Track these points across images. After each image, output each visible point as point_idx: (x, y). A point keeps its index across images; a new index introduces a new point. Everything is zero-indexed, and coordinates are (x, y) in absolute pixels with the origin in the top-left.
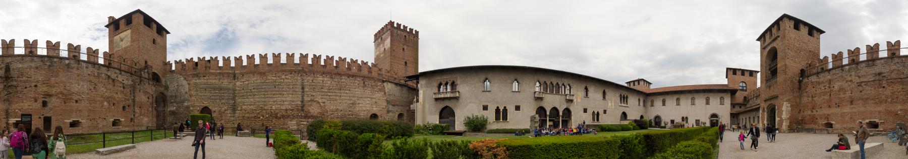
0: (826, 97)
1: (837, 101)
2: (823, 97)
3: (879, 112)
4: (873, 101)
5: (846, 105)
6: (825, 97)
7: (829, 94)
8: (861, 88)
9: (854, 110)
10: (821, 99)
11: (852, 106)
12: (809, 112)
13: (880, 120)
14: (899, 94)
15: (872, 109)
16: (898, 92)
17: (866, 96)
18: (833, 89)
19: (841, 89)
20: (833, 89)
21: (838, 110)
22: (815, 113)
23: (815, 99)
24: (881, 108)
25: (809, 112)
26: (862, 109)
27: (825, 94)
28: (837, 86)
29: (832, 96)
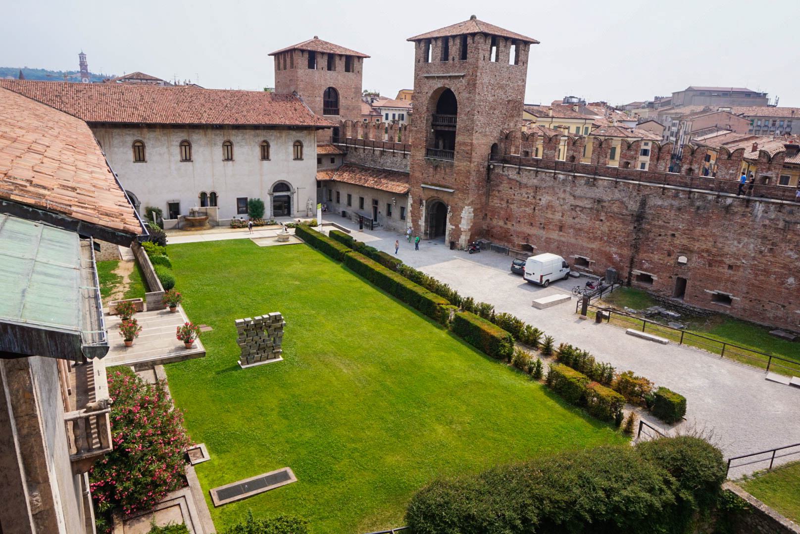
0: (529, 210)
1: (543, 221)
2: (523, 208)
3: (592, 250)
4: (586, 235)
5: (553, 230)
6: (527, 209)
7: (532, 207)
8: (574, 213)
9: (563, 239)
10: (521, 209)
11: (561, 233)
12: (501, 223)
13: (592, 259)
15: (585, 244)
17: (578, 226)
18: (538, 201)
19: (549, 206)
20: (538, 201)
21: (542, 233)
22: (509, 226)
23: (512, 206)
24: (595, 245)
25: (501, 223)
26: (573, 241)
27: (528, 204)
28: (545, 199)
29: (537, 211)
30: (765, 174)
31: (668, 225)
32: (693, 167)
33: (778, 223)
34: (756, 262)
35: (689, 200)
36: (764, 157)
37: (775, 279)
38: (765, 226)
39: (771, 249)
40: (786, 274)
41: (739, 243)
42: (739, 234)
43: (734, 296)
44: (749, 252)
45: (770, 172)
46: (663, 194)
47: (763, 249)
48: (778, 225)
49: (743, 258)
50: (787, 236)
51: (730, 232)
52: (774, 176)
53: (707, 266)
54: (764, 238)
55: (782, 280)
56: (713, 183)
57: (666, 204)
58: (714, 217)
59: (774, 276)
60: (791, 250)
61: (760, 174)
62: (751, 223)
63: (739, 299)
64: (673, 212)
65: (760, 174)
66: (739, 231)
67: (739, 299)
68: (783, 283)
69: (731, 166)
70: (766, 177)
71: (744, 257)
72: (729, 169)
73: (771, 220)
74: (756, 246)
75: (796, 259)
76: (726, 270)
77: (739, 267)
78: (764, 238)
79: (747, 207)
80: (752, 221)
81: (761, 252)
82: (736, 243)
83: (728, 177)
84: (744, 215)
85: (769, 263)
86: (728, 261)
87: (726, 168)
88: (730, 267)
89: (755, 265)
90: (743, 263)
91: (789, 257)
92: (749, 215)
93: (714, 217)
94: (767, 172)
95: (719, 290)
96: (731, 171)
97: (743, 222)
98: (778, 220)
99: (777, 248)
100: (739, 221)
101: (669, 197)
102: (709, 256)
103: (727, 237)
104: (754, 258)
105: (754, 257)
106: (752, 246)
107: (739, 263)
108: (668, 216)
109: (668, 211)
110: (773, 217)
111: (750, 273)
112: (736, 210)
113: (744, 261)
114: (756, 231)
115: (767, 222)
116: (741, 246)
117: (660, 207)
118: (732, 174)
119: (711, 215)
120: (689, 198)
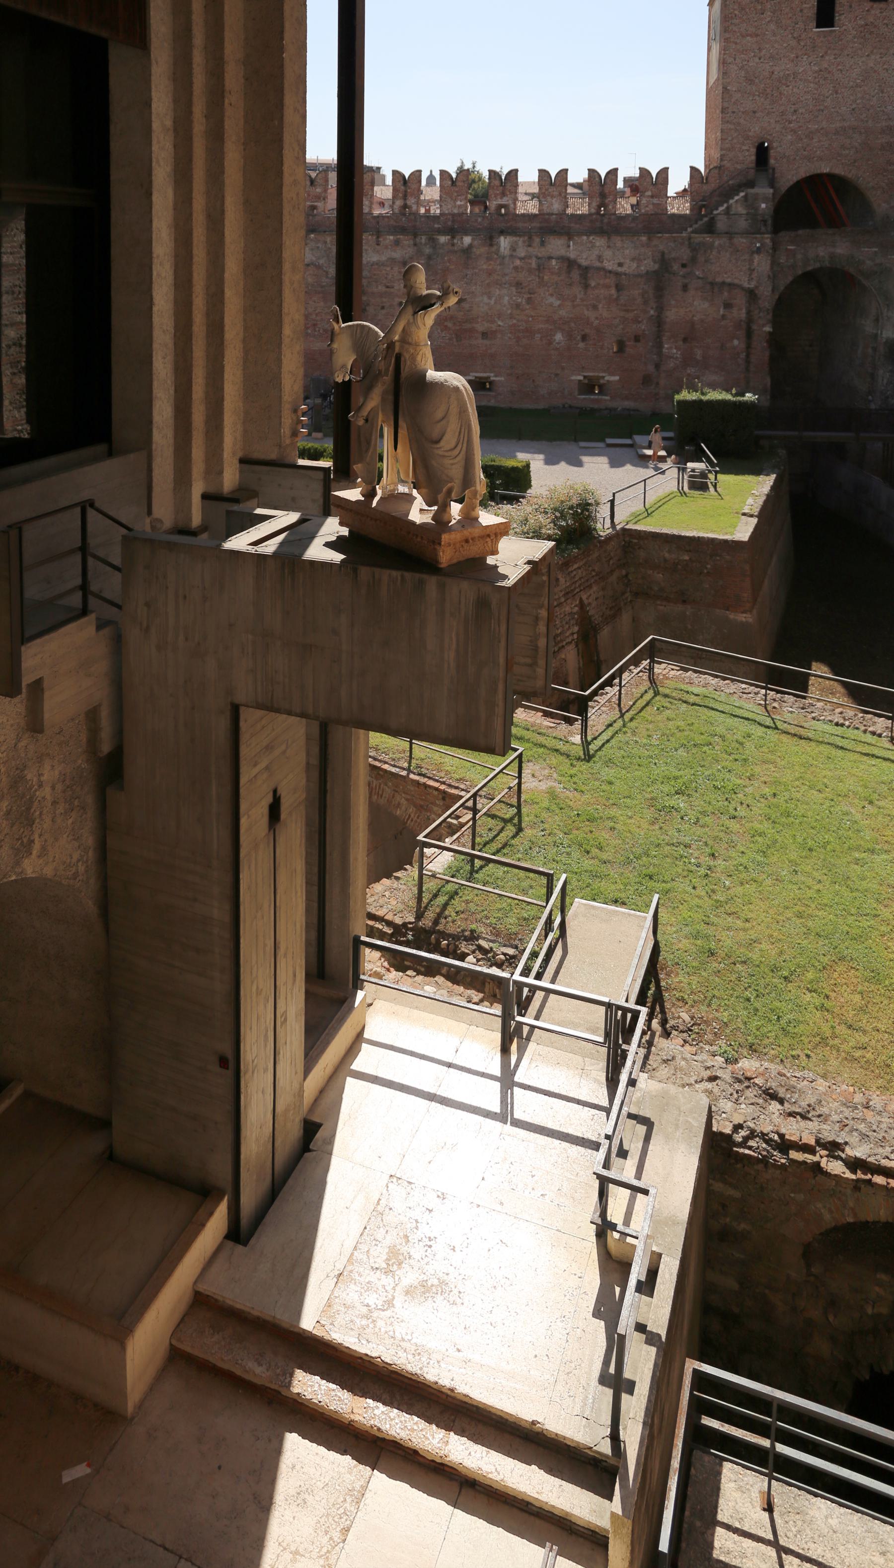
14: (318, 318)
16: (317, 315)
30: (500, 202)
31: (392, 290)
32: (408, 203)
33: (530, 261)
34: (515, 321)
35: (415, 248)
36: (495, 179)
37: (541, 340)
38: (516, 268)
39: (528, 298)
40: (551, 330)
41: (490, 298)
42: (488, 284)
43: (496, 376)
44: (505, 309)
45: (505, 199)
46: (378, 244)
47: (520, 300)
48: (531, 264)
49: (499, 318)
50: (543, 277)
51: (476, 284)
52: (510, 202)
53: (455, 340)
54: (518, 284)
55: (549, 338)
56: (438, 223)
57: (384, 258)
58: (452, 267)
59: (539, 336)
60: (552, 295)
61: (495, 203)
62: (499, 267)
63: (503, 379)
64: (396, 269)
65: (495, 203)
66: (487, 282)
67: (503, 379)
68: (550, 343)
69: (458, 196)
70: (501, 206)
71: (500, 316)
72: (455, 200)
73: (521, 259)
74: (511, 298)
75: (559, 306)
76: (480, 341)
77: (496, 331)
78: (518, 284)
79: (491, 245)
80: (500, 264)
81: (518, 306)
82: (486, 299)
83: (456, 211)
84: (489, 259)
85: (530, 319)
86: (480, 327)
87: (452, 199)
88: (484, 335)
89: (514, 325)
90: (499, 326)
91: (551, 305)
92: (495, 256)
93: (452, 267)
94: (501, 198)
95: (476, 372)
96: (459, 203)
97: (490, 267)
98: (530, 257)
99: (536, 295)
100: (485, 267)
101: (386, 247)
102: (454, 324)
103: (473, 292)
104: (511, 317)
105: (511, 314)
106: (507, 298)
107: (494, 327)
108: (390, 276)
109: (388, 269)
110: (523, 255)
111: (510, 338)
112: (478, 253)
113: (500, 323)
114: (507, 278)
115: (518, 262)
116: (492, 302)
117: (377, 264)
118: (460, 206)
119: (448, 264)
120: (415, 245)
